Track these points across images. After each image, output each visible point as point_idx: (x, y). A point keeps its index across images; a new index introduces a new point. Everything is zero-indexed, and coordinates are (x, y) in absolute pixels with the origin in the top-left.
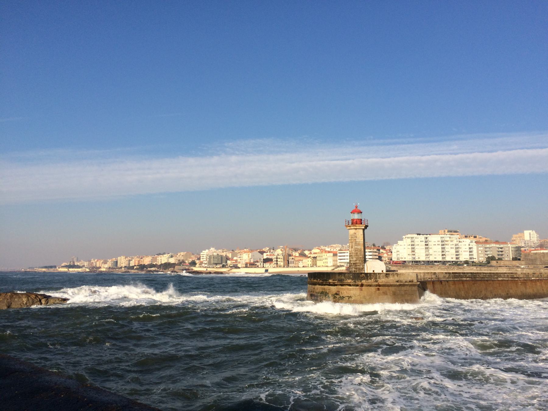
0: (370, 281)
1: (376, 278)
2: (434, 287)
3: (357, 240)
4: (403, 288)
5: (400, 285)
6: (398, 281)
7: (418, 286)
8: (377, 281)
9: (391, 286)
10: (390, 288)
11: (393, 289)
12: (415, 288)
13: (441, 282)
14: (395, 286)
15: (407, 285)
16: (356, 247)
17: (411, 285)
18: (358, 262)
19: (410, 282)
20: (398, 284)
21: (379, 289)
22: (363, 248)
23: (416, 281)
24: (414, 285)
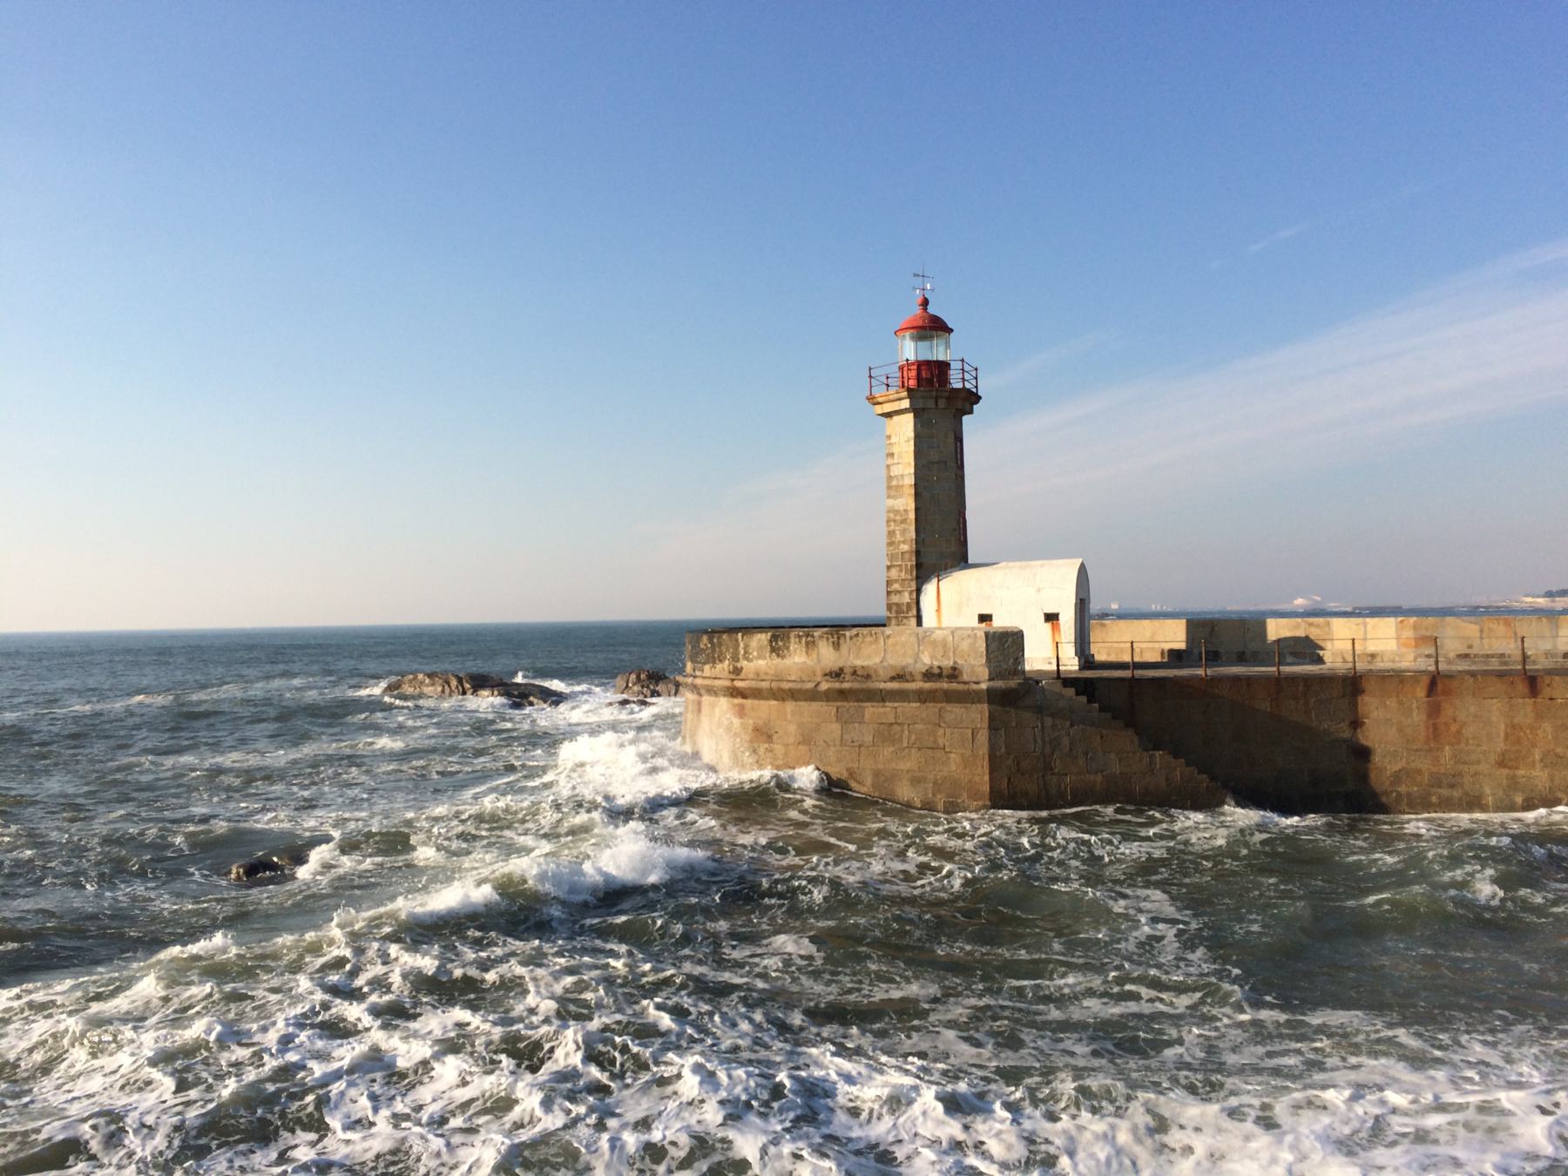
0: (719, 666)
1: (735, 658)
2: (1434, 711)
3: (895, 471)
4: (871, 710)
5: (842, 694)
6: (837, 674)
7: (993, 696)
8: (737, 671)
9: (794, 695)
10: (790, 706)
11: (810, 709)
12: (978, 715)
13: (1533, 683)
14: (812, 695)
15: (902, 696)
16: (890, 502)
17: (923, 697)
18: (894, 573)
19: (929, 675)
20: (824, 686)
21: (742, 707)
22: (912, 506)
23: (984, 673)
24: (965, 697)
